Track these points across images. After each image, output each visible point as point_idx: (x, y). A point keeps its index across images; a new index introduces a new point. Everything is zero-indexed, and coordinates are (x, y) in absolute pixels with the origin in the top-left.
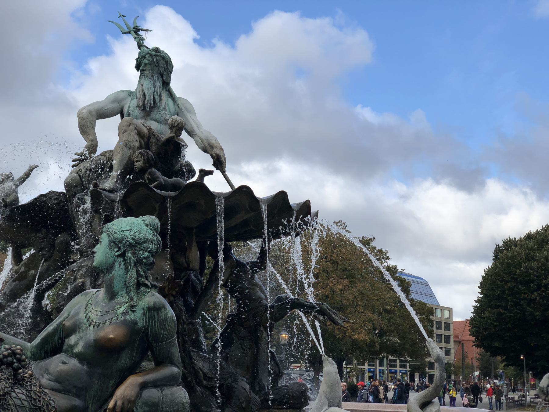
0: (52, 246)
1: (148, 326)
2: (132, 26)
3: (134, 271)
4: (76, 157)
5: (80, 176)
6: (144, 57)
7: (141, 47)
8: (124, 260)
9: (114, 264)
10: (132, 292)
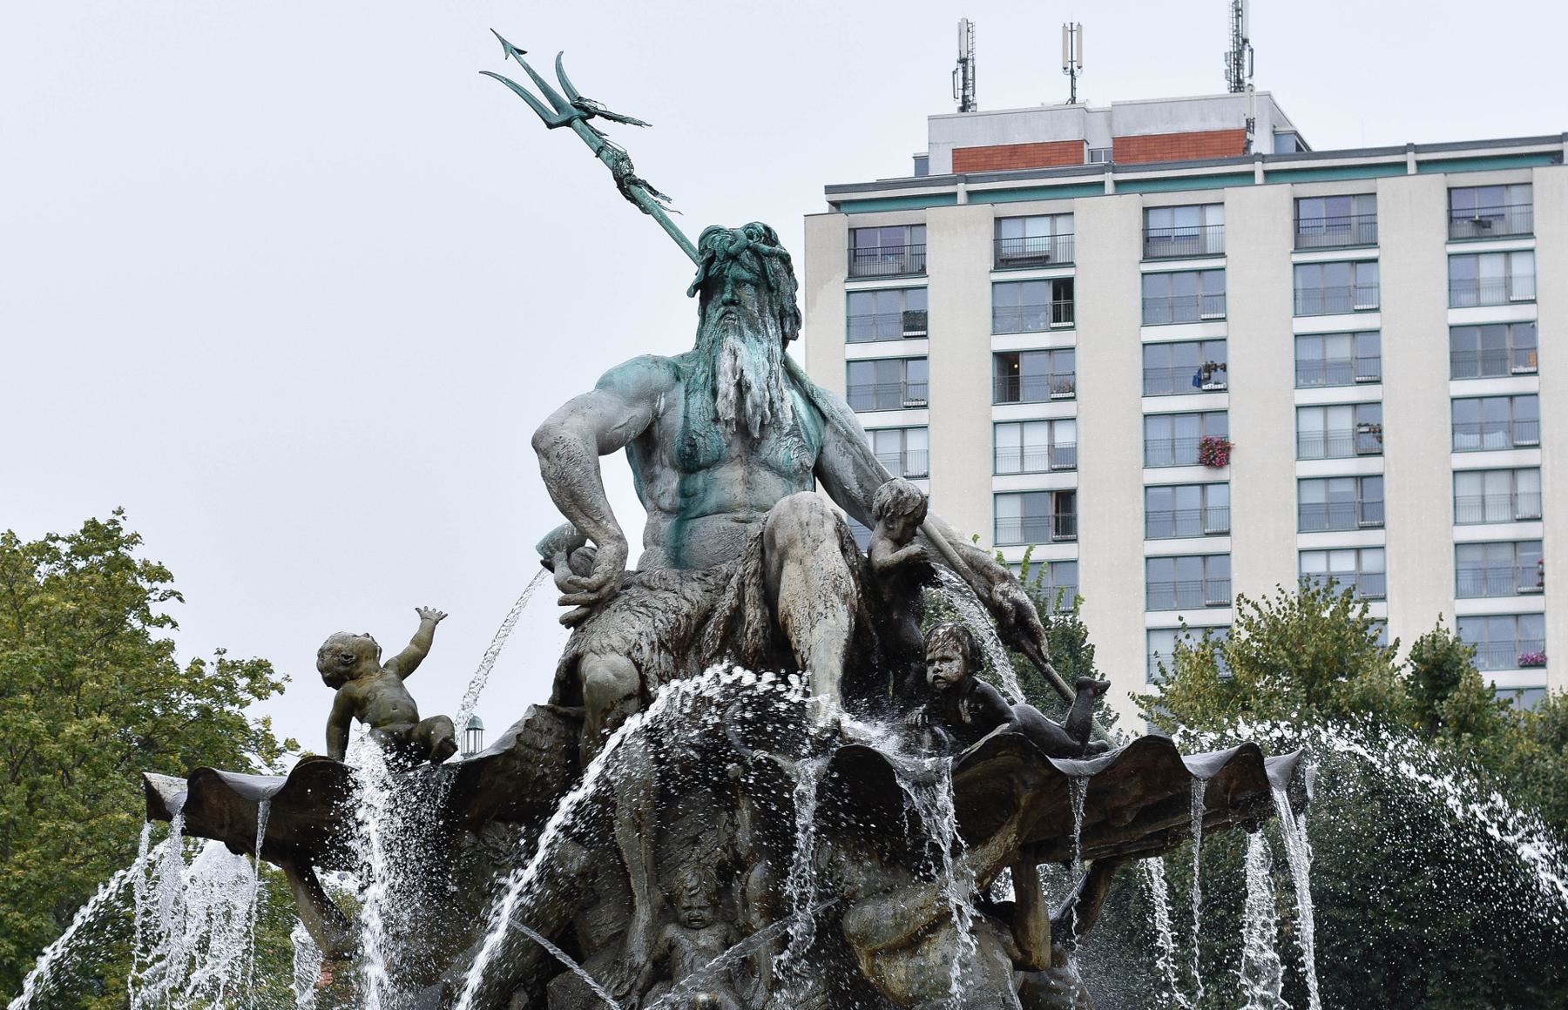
5: (638, 666)
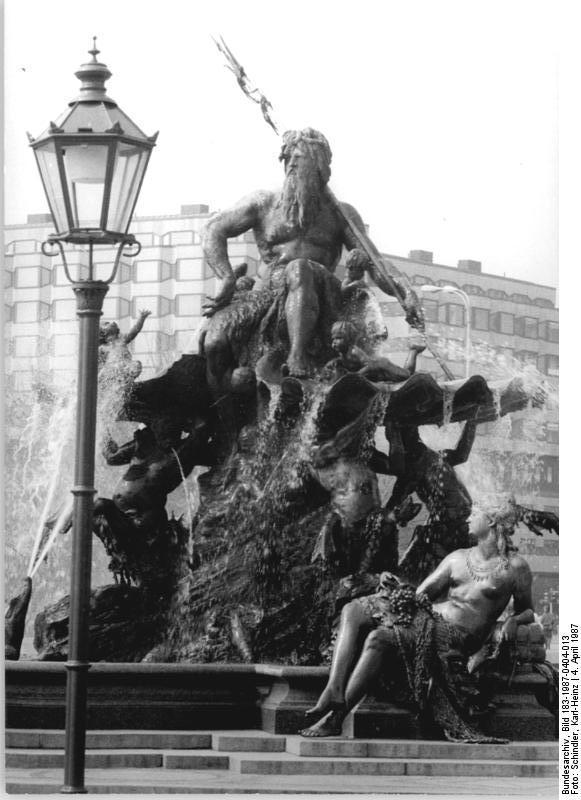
4: (210, 303)
6: (295, 145)
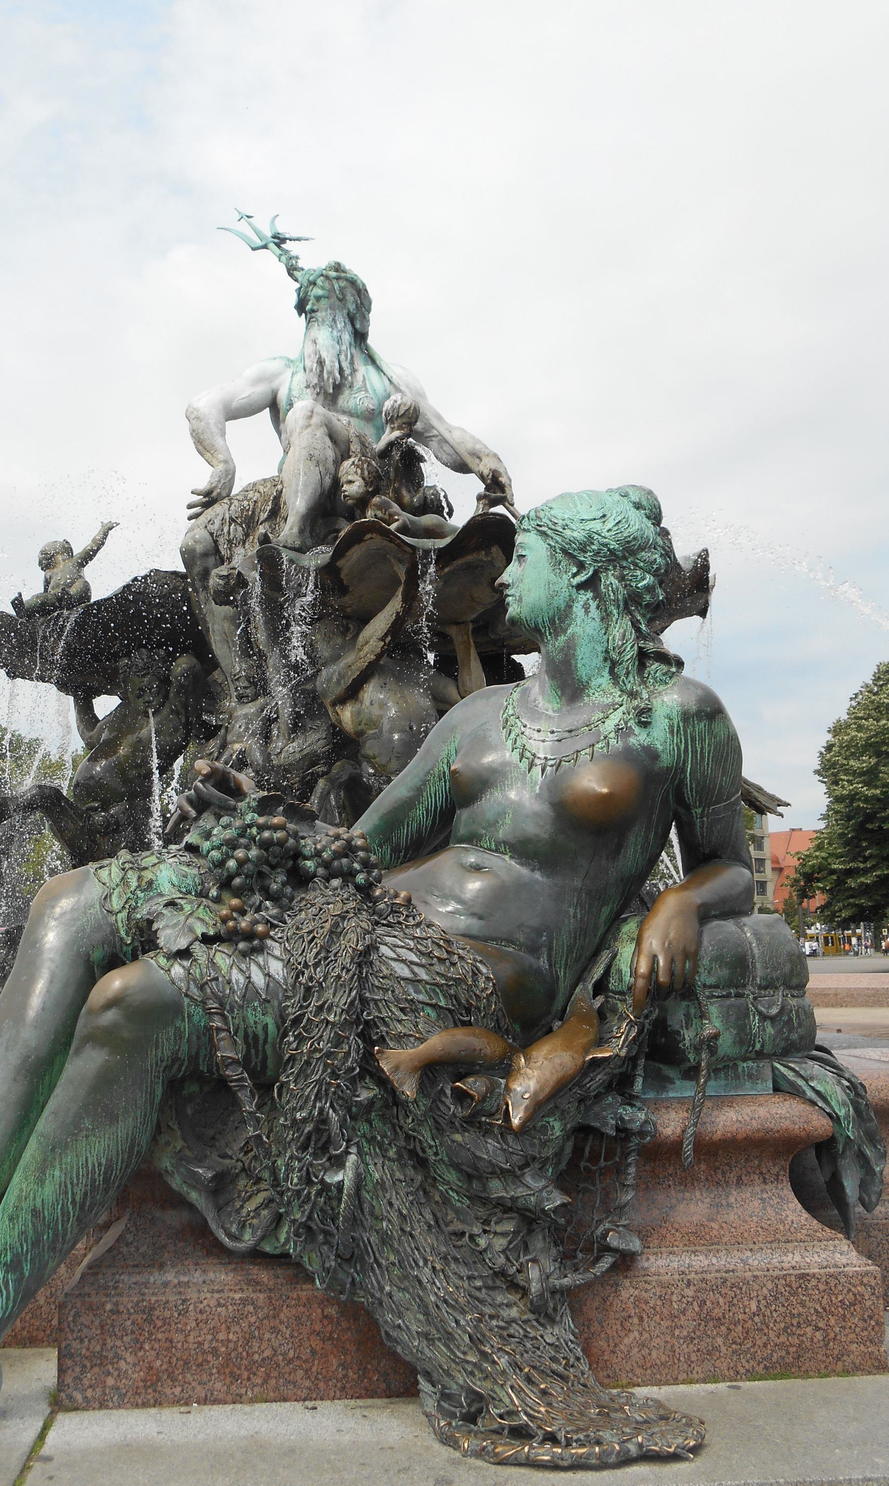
0: (165, 681)
1: (685, 762)
2: (269, 234)
3: (626, 622)
7: (295, 273)
8: (598, 596)
9: (571, 607)
10: (631, 678)
